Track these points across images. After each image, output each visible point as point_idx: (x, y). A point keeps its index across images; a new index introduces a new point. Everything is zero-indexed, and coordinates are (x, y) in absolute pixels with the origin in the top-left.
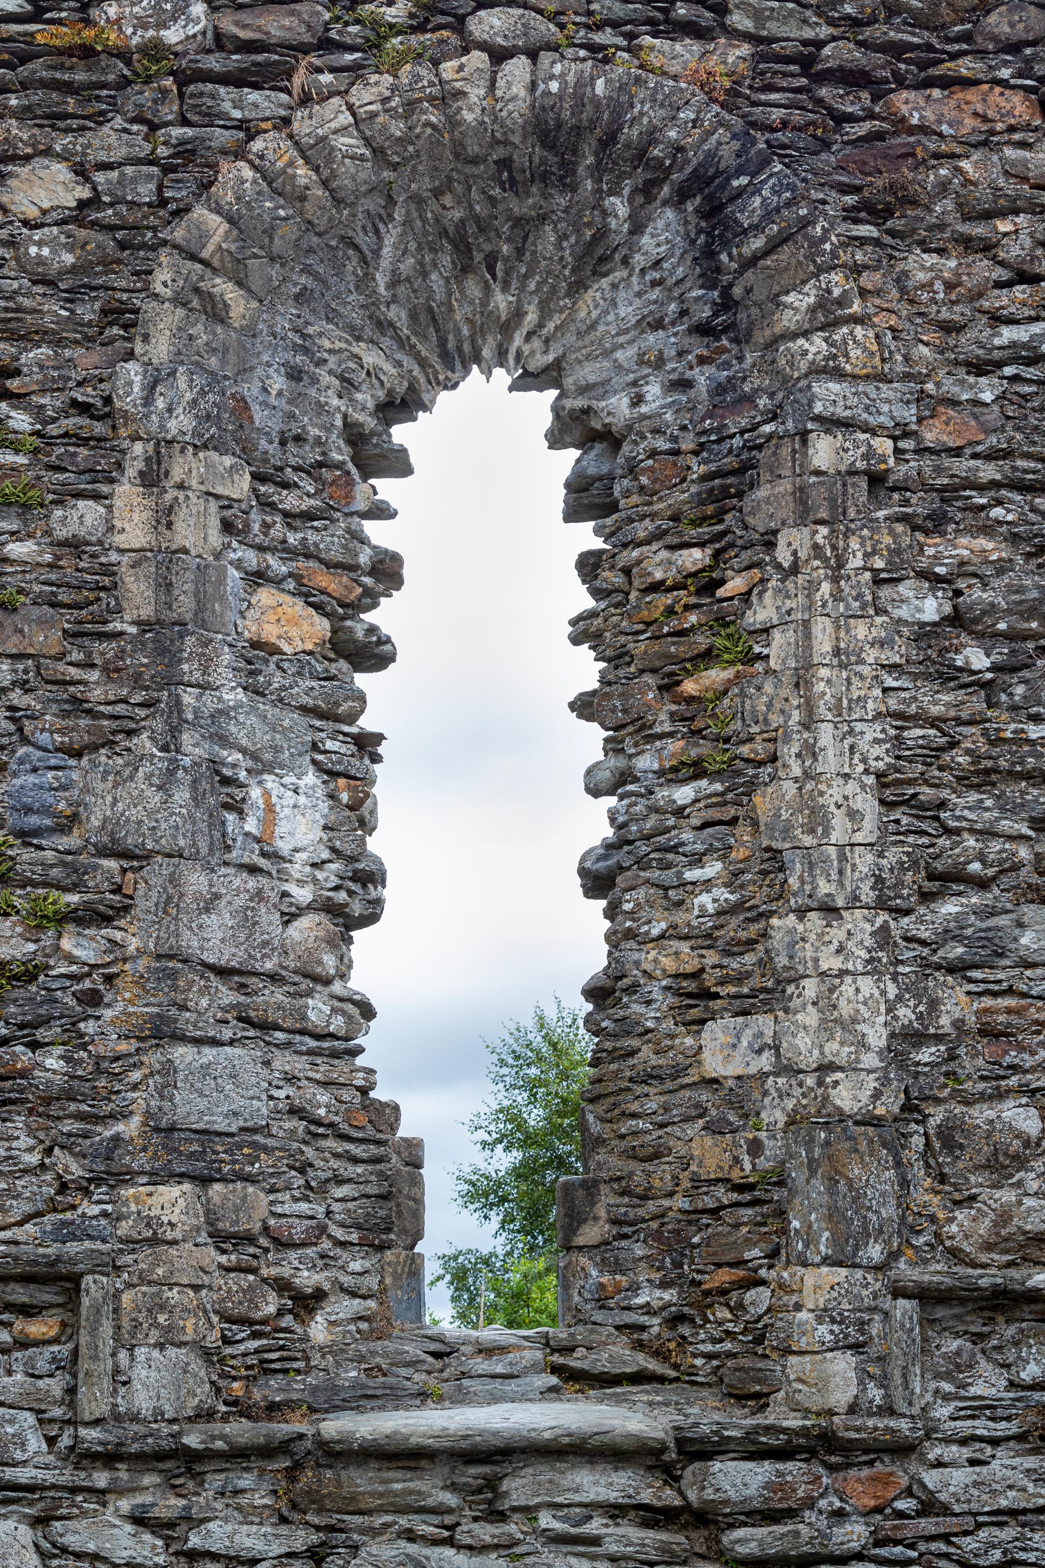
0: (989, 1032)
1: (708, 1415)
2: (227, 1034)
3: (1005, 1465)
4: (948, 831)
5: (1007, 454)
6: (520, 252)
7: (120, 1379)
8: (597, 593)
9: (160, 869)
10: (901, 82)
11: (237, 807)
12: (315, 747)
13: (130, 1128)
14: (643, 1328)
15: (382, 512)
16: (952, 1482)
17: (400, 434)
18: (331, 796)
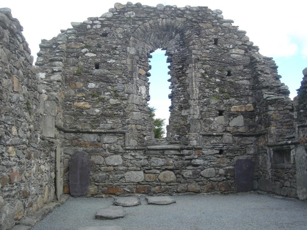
0: (209, 111)
1: (183, 146)
2: (138, 111)
3: (209, 150)
4: (205, 93)
5: (210, 58)
6: (164, 37)
8: (170, 70)
9: (131, 95)
10: (200, 23)
11: (138, 89)
12: (145, 84)
14: (175, 139)
15: (150, 62)
16: (205, 152)
17: (151, 54)
18: (146, 89)
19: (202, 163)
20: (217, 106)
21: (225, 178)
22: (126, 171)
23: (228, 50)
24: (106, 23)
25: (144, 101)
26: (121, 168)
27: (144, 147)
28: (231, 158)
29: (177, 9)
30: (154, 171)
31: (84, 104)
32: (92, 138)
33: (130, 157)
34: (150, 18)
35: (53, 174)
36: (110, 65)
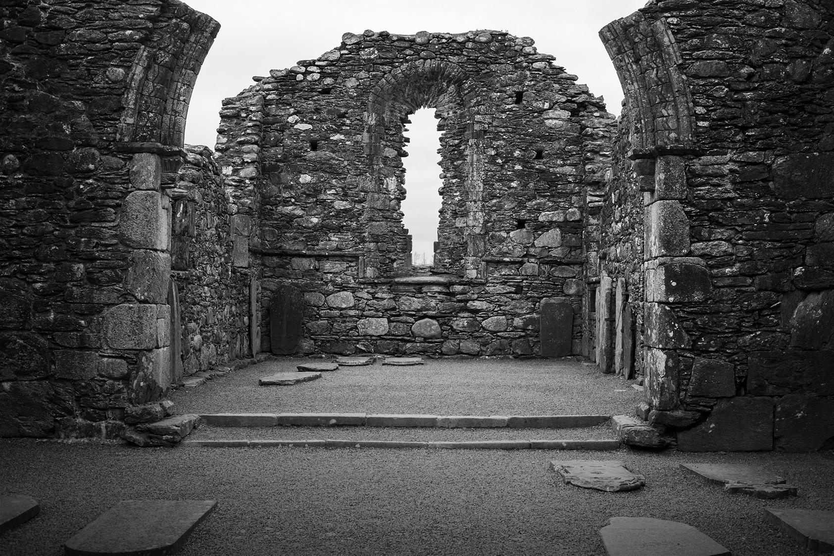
3: (498, 286)
7: (365, 272)
9: (370, 194)
13: (366, 234)
15: (406, 130)
16: (490, 289)
17: (410, 117)
19: (485, 307)
20: (515, 212)
21: (523, 334)
22: (360, 317)
23: (541, 111)
24: (328, 70)
25: (393, 202)
26: (352, 313)
27: (389, 280)
28: (535, 301)
29: (452, 39)
30: (404, 318)
31: (294, 210)
32: (307, 264)
33: (366, 296)
34: (404, 58)
35: (246, 319)
36: (336, 143)
